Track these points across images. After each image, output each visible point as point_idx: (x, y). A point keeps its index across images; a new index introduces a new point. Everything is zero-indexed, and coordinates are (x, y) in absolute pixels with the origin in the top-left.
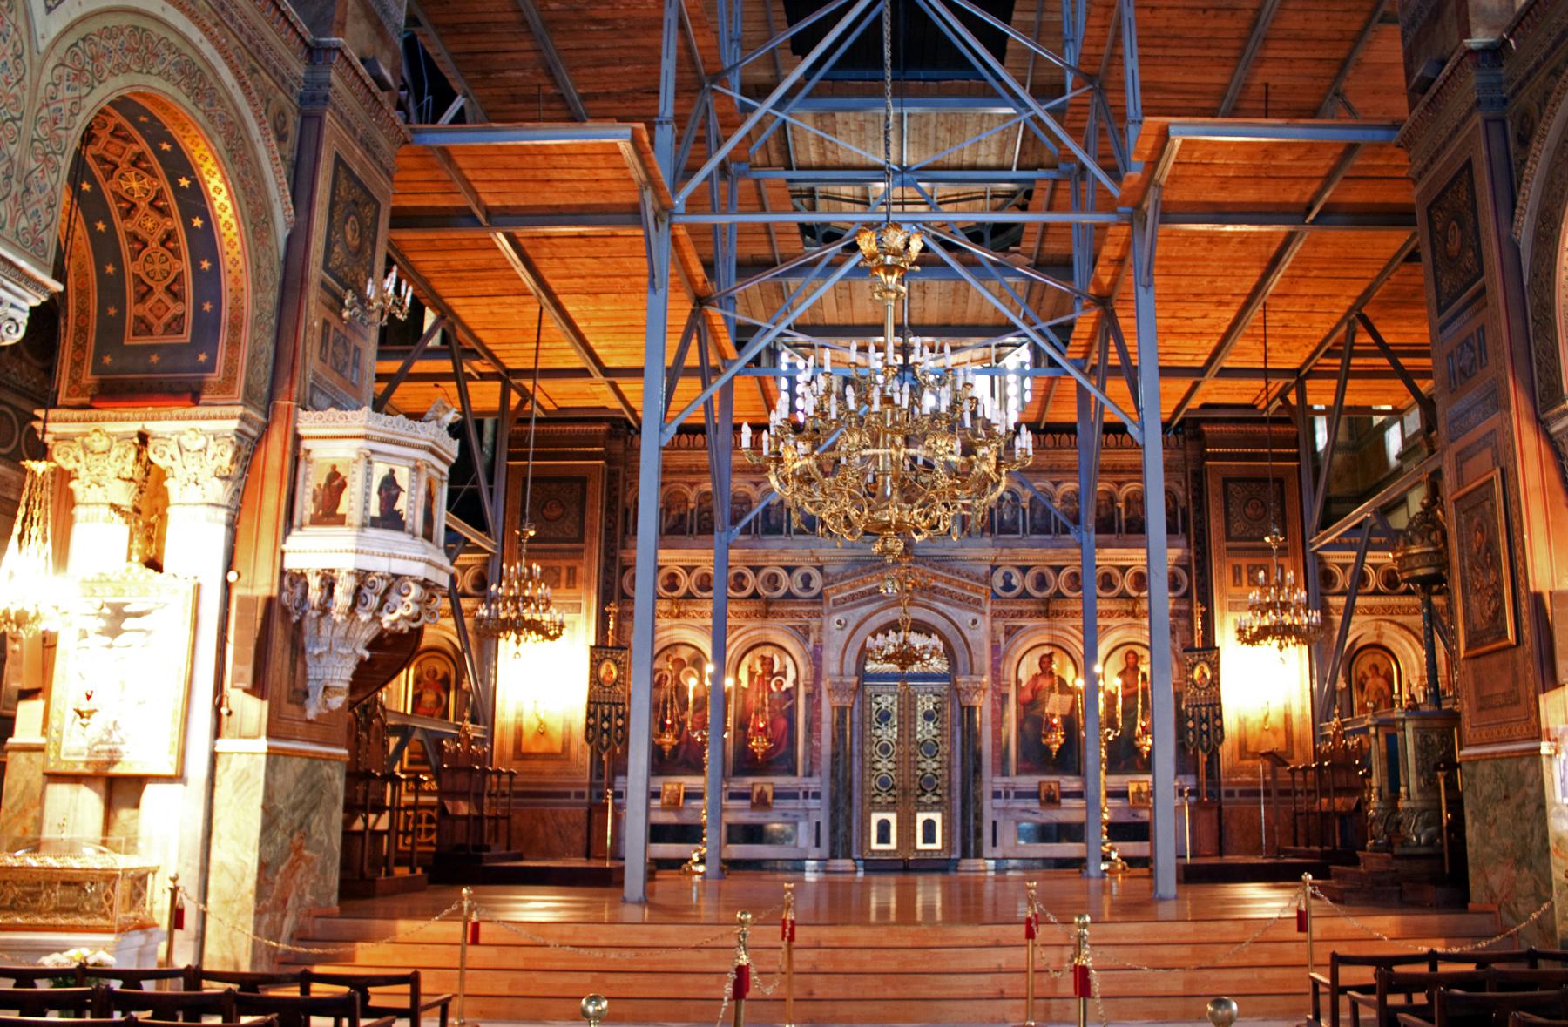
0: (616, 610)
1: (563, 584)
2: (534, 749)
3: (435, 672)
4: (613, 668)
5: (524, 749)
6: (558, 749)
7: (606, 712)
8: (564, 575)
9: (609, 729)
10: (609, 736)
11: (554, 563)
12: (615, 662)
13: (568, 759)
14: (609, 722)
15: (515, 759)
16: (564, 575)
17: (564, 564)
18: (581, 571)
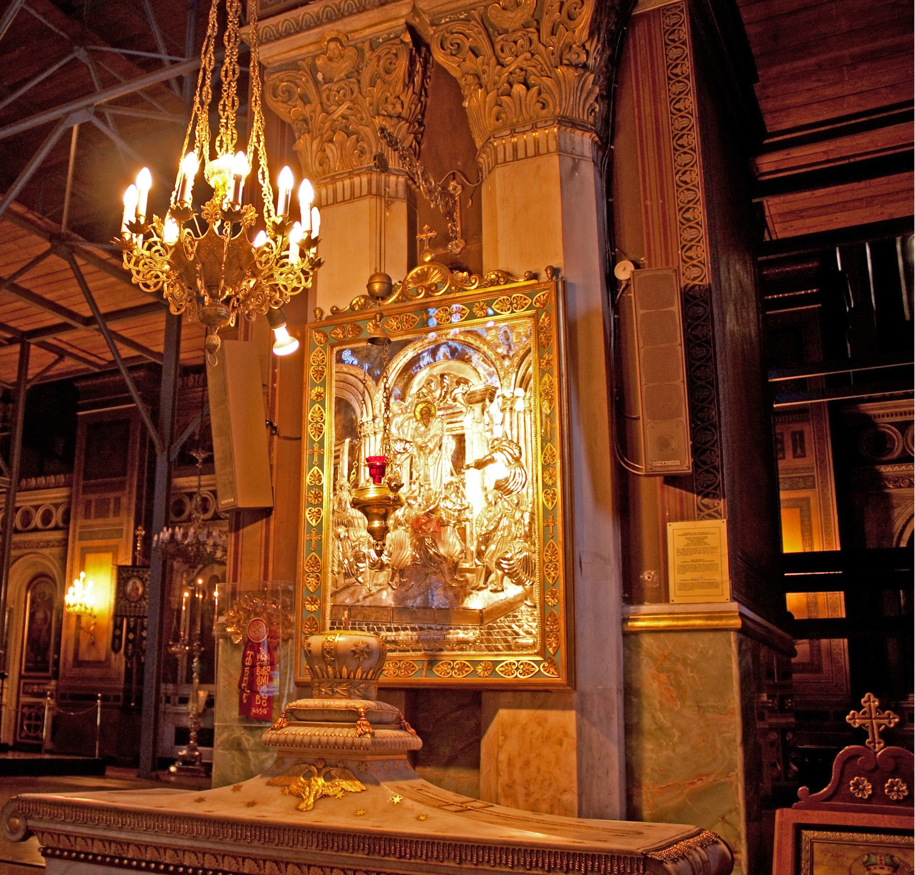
0: (143, 533)
1: (111, 513)
2: (87, 658)
3: (44, 593)
4: (139, 584)
5: (81, 658)
6: (103, 658)
7: (132, 624)
8: (112, 506)
9: (134, 639)
10: (134, 645)
11: (107, 495)
12: (141, 579)
13: (109, 667)
14: (135, 633)
15: (74, 666)
16: (112, 506)
17: (112, 495)
18: (124, 500)
